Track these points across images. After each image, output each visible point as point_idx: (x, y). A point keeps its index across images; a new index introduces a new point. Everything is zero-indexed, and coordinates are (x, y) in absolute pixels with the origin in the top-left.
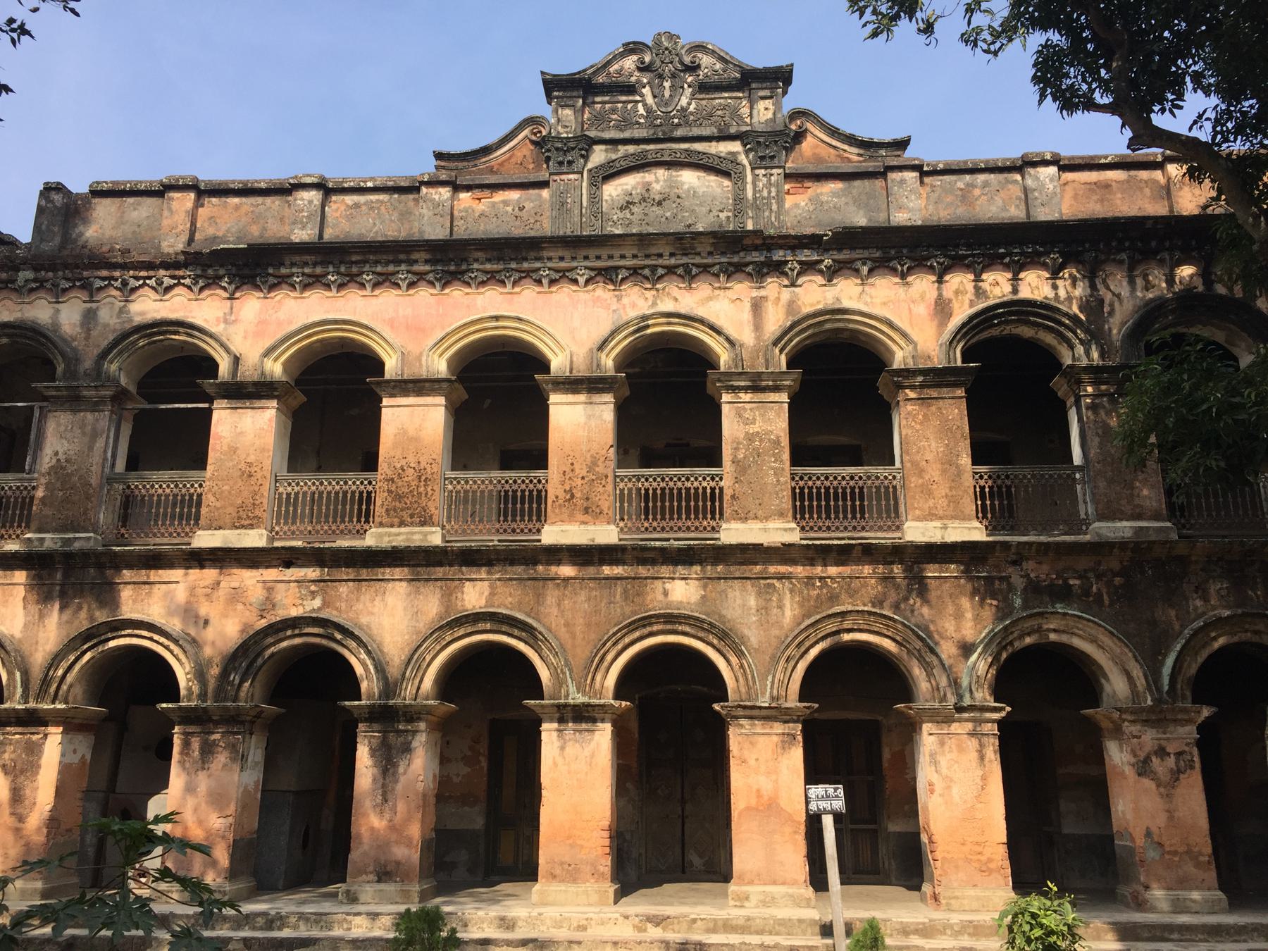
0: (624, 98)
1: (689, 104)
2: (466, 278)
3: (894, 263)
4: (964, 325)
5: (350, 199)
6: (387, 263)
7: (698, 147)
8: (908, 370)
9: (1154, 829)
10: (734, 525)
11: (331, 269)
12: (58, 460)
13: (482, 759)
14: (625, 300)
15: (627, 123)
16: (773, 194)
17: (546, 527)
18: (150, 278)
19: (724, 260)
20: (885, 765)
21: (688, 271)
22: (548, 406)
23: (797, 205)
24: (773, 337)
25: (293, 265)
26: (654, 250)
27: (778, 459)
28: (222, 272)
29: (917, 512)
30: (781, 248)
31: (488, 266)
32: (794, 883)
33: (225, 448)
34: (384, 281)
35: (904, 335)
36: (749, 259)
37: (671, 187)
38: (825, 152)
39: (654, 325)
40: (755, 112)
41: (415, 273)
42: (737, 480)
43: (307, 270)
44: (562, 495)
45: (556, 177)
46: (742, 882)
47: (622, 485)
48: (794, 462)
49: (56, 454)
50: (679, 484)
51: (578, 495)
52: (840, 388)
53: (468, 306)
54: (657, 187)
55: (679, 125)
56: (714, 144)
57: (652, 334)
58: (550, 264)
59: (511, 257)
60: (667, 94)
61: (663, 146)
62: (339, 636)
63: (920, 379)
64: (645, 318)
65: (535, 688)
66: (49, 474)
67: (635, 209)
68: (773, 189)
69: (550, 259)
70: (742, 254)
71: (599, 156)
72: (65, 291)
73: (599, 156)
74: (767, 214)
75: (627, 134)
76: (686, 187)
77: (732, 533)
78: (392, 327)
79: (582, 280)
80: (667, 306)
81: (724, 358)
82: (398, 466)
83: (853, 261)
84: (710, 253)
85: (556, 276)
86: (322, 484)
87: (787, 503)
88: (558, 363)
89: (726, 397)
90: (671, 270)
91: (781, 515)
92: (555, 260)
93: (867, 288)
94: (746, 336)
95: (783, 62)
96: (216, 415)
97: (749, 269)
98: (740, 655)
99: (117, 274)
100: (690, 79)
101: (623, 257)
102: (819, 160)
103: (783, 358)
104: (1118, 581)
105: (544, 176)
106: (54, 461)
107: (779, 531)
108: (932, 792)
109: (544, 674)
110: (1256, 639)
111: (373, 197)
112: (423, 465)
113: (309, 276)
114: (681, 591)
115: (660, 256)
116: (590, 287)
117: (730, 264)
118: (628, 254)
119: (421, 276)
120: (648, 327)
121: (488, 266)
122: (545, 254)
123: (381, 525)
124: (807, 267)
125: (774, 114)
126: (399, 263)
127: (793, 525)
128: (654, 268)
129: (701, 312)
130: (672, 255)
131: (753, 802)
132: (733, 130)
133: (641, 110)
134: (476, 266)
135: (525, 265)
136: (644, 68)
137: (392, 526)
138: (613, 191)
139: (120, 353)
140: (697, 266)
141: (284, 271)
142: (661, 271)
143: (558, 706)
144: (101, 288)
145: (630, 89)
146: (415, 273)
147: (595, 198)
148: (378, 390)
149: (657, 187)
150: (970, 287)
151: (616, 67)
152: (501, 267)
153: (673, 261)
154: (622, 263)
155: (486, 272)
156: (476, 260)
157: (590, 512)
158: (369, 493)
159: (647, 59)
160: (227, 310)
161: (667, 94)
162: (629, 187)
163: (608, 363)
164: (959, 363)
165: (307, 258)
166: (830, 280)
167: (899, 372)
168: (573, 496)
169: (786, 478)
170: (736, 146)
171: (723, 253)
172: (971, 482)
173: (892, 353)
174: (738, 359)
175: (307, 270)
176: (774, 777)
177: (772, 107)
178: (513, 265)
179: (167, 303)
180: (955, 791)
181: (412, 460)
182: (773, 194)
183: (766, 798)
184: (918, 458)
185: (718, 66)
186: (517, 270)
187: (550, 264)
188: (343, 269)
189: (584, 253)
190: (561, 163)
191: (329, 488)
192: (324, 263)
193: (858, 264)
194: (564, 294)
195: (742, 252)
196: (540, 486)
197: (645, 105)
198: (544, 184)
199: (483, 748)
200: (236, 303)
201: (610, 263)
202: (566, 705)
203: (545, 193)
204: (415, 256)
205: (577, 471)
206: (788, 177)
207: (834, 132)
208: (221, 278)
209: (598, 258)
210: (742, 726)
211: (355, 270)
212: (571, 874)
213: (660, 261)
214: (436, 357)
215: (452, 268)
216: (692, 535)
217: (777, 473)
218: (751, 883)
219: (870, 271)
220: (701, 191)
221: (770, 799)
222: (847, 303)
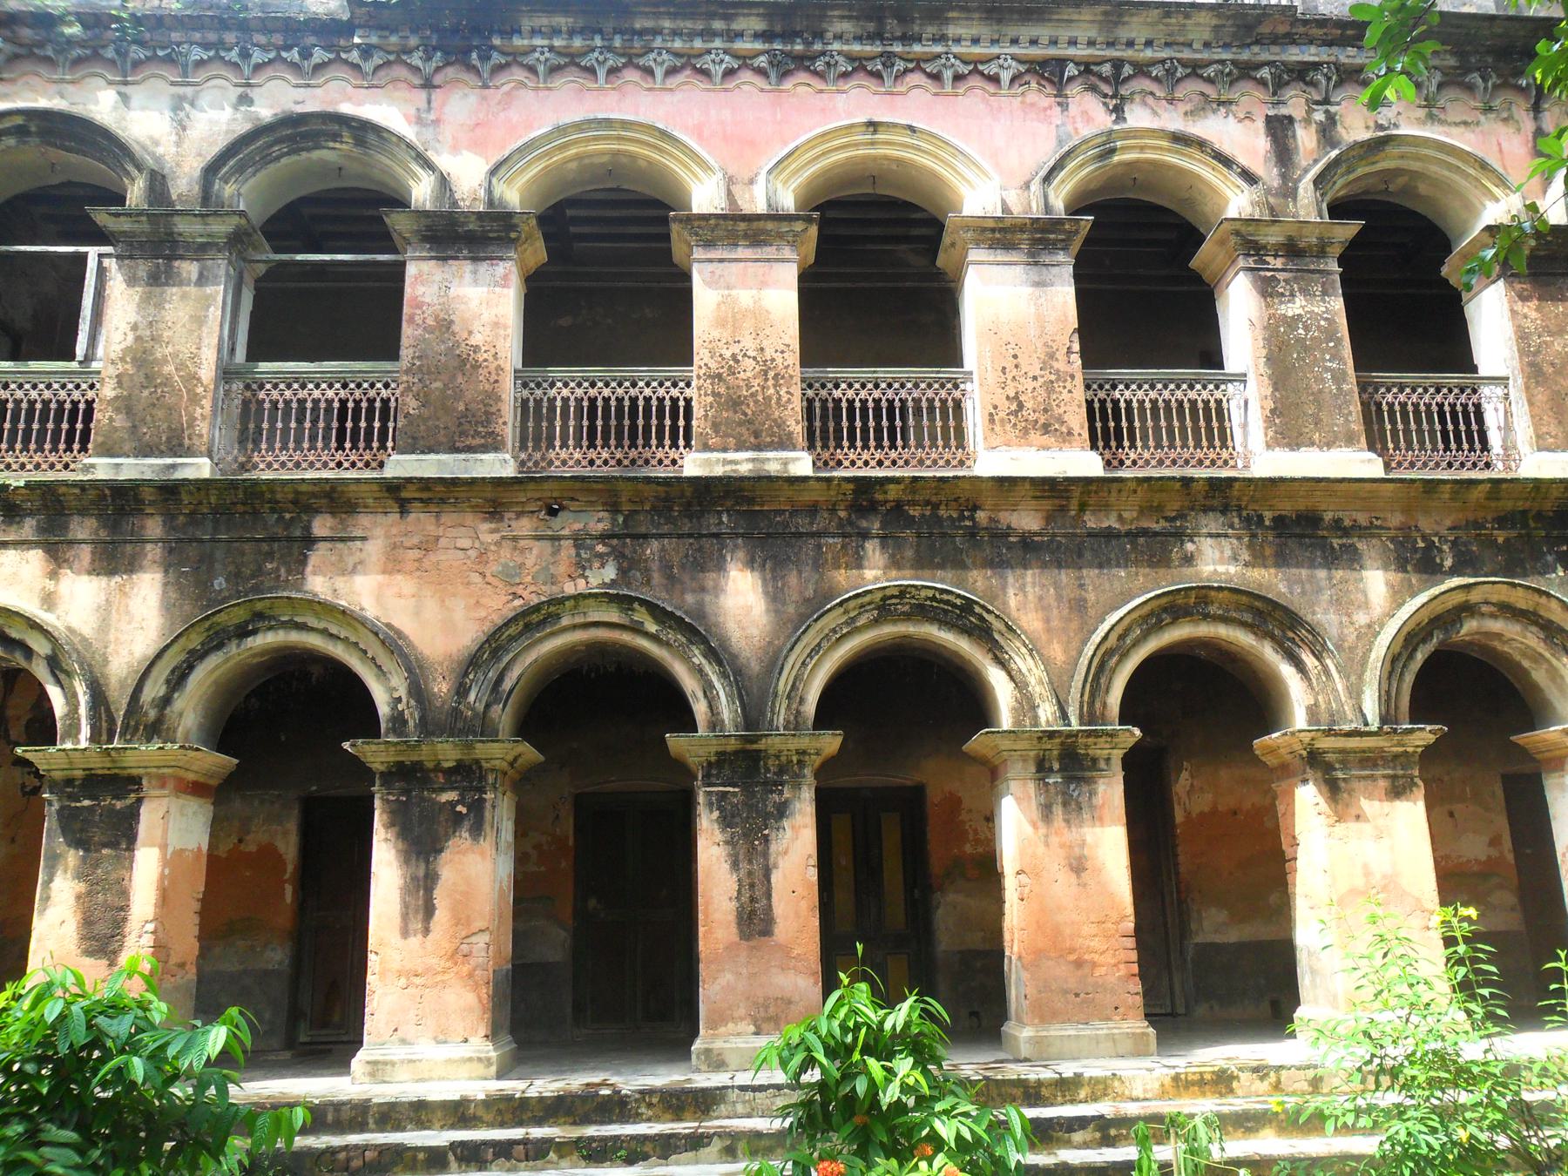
2: (819, 65)
6: (692, 35)
11: (598, 42)
12: (138, 339)
14: (1073, 108)
18: (288, 48)
19: (1224, 56)
21: (1170, 73)
25: (534, 32)
28: (413, 41)
31: (856, 48)
33: (430, 322)
34: (683, 67)
36: (1265, 56)
49: (135, 327)
51: (1029, 405)
53: (823, 110)
57: (1120, 164)
58: (956, 49)
62: (652, 627)
66: (122, 359)
69: (958, 40)
70: (1256, 49)
72: (137, 64)
79: (1006, 76)
82: (728, 354)
84: (1207, 45)
85: (965, 69)
91: (1350, 440)
96: (412, 270)
97: (1265, 73)
99: (230, 37)
101: (1073, 42)
103: (1324, 206)
106: (131, 337)
112: (769, 354)
113: (558, 53)
118: (1083, 39)
119: (745, 60)
120: (1113, 151)
121: (856, 48)
122: (952, 31)
123: (706, 448)
126: (708, 34)
128: (1118, 64)
130: (1149, 43)
131: (1360, 882)
134: (836, 46)
135: (917, 48)
137: (725, 450)
139: (240, 169)
141: (518, 42)
142: (1127, 70)
144: (200, 63)
146: (736, 56)
154: (1071, 51)
155: (851, 58)
156: (839, 37)
160: (424, 105)
168: (1021, 406)
171: (1226, 46)
175: (558, 42)
178: (897, 48)
179: (318, 91)
181: (749, 344)
183: (1378, 876)
187: (956, 49)
188: (617, 42)
189: (1012, 31)
194: (974, 100)
200: (437, 95)
201: (1053, 52)
208: (409, 52)
209: (1034, 42)
214: (779, 186)
215: (799, 47)
221: (1385, 877)
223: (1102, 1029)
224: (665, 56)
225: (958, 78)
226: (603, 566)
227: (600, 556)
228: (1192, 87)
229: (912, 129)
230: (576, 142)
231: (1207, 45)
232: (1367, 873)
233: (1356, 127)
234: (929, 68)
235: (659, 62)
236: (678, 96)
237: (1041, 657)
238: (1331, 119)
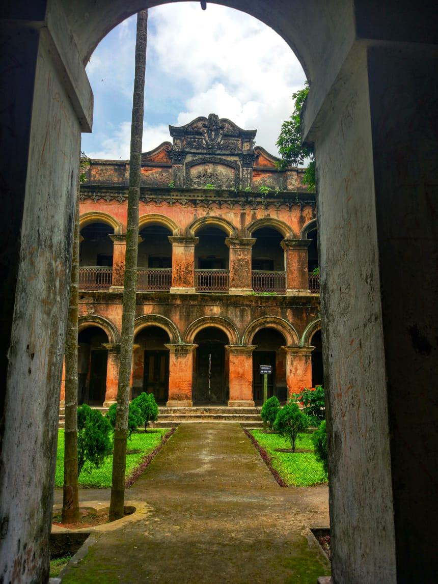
0: (198, 137)
1: (221, 141)
3: (287, 204)
4: (308, 226)
5: (100, 168)
7: (224, 157)
8: (290, 240)
10: (233, 289)
11: (95, 194)
13: (142, 364)
15: (199, 146)
16: (249, 177)
17: (171, 288)
20: (276, 365)
23: (257, 181)
24: (248, 227)
26: (209, 195)
27: (248, 268)
29: (291, 286)
30: (251, 197)
31: (151, 197)
32: (249, 400)
35: (290, 228)
36: (240, 200)
37: (214, 171)
38: (266, 162)
39: (208, 220)
40: (244, 147)
41: (125, 197)
42: (234, 274)
43: (86, 194)
44: (176, 276)
45: (175, 165)
46: (232, 399)
47: (196, 274)
48: (252, 269)
50: (215, 274)
52: (268, 243)
54: (210, 171)
55: (217, 149)
56: (229, 157)
59: (159, 193)
60: (213, 137)
61: (212, 156)
63: (294, 243)
64: (205, 218)
65: (168, 340)
67: (202, 178)
68: (249, 175)
69: (173, 195)
70: (238, 198)
71: (189, 158)
73: (189, 158)
74: (247, 183)
75: (199, 151)
76: (219, 171)
77: (233, 291)
78: (117, 216)
79: (184, 203)
80: (212, 214)
81: (231, 233)
83: (274, 202)
85: (174, 201)
86: (92, 270)
87: (250, 282)
88: (175, 231)
89: (231, 247)
90: (214, 202)
91: (248, 286)
92: (174, 196)
93: (279, 212)
94: (239, 226)
95: (254, 129)
97: (241, 203)
98: (234, 330)
100: (221, 132)
101: (198, 196)
102: (264, 165)
103: (251, 234)
105: (170, 164)
107: (247, 291)
108: (291, 372)
109: (171, 336)
111: (108, 167)
113: (86, 196)
114: (216, 310)
115: (211, 197)
116: (187, 206)
117: (234, 201)
118: (200, 195)
120: (206, 221)
121: (151, 197)
122: (171, 194)
123: (114, 285)
124: (259, 203)
125: (250, 148)
127: (252, 289)
129: (224, 217)
130: (215, 197)
132: (236, 153)
133: (204, 142)
135: (164, 197)
136: (205, 126)
137: (118, 286)
138: (194, 171)
140: (223, 201)
142: (211, 202)
143: (175, 346)
145: (201, 134)
146: (125, 197)
147: (188, 173)
148: (112, 238)
149: (210, 171)
150: (311, 213)
151: (195, 125)
152: (155, 197)
153: (215, 199)
156: (147, 194)
157: (186, 283)
158: (109, 274)
159: (207, 123)
161: (213, 137)
162: (200, 170)
163: (192, 232)
164: (306, 239)
165: (86, 190)
166: (266, 208)
167: (287, 241)
168: (180, 278)
169: (250, 274)
170: (236, 159)
171: (232, 197)
172: (308, 277)
173: (285, 234)
174: (236, 235)
175: (86, 194)
176: (243, 368)
177: (249, 145)
182: (249, 177)
184: (292, 269)
185: (231, 128)
186: (161, 198)
189: (184, 194)
190: (176, 160)
191: (95, 271)
192: (92, 192)
193: (276, 204)
194: (177, 208)
195: (239, 197)
196: (169, 274)
197: (205, 140)
198: (171, 167)
199: (143, 360)
201: (193, 198)
202: (178, 346)
203: (170, 170)
204: (125, 191)
205: (182, 269)
206: (254, 170)
207: (270, 156)
209: (190, 196)
210: (234, 352)
211: (103, 195)
212: (178, 398)
213: (211, 199)
216: (219, 291)
217: (247, 272)
218: (235, 400)
219: (280, 206)
220: (224, 173)
222: (272, 217)
223: (182, 402)
224: (109, 197)
225: (173, 203)
226: (92, 309)
227: (91, 307)
228: (225, 205)
229: (162, 216)
230: (89, 217)
231: (227, 197)
232: (238, 373)
233: (260, 215)
234: (167, 201)
235: (108, 198)
236: (112, 206)
237: (181, 330)
238: (255, 213)
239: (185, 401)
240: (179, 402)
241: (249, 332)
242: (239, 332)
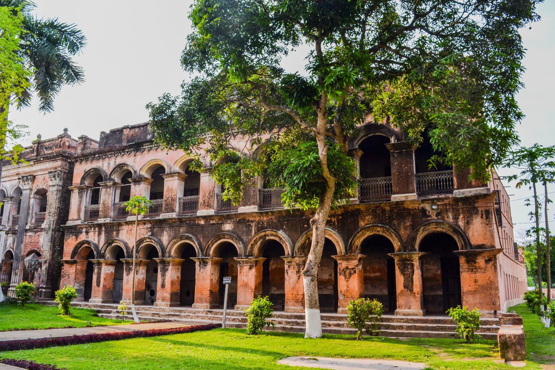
9: (343, 291)
10: (243, 207)
22: (200, 177)
44: (203, 202)
104: (340, 217)
110: (378, 233)
157: (209, 206)
180: (291, 280)
232: (244, 282)
239: (205, 304)
240: (201, 304)
241: (252, 245)
242: (249, 244)
